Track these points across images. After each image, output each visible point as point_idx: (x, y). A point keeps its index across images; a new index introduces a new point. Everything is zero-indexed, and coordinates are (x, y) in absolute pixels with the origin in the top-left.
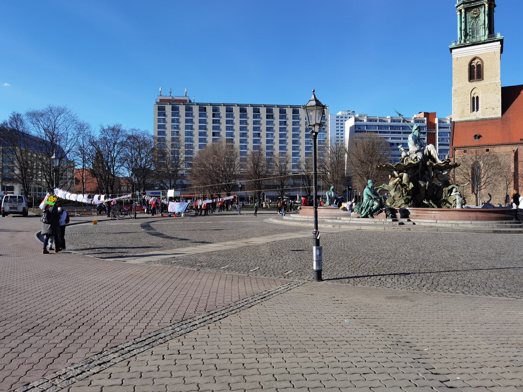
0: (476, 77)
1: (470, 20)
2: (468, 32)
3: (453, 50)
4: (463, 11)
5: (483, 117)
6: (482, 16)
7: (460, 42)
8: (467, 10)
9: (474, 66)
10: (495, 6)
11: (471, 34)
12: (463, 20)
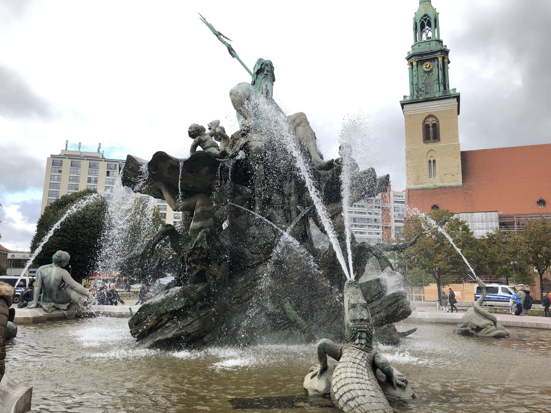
1: (422, 74)
3: (405, 106)
4: (415, 63)
5: (441, 185)
10: (449, 62)
11: (423, 89)
12: (415, 73)
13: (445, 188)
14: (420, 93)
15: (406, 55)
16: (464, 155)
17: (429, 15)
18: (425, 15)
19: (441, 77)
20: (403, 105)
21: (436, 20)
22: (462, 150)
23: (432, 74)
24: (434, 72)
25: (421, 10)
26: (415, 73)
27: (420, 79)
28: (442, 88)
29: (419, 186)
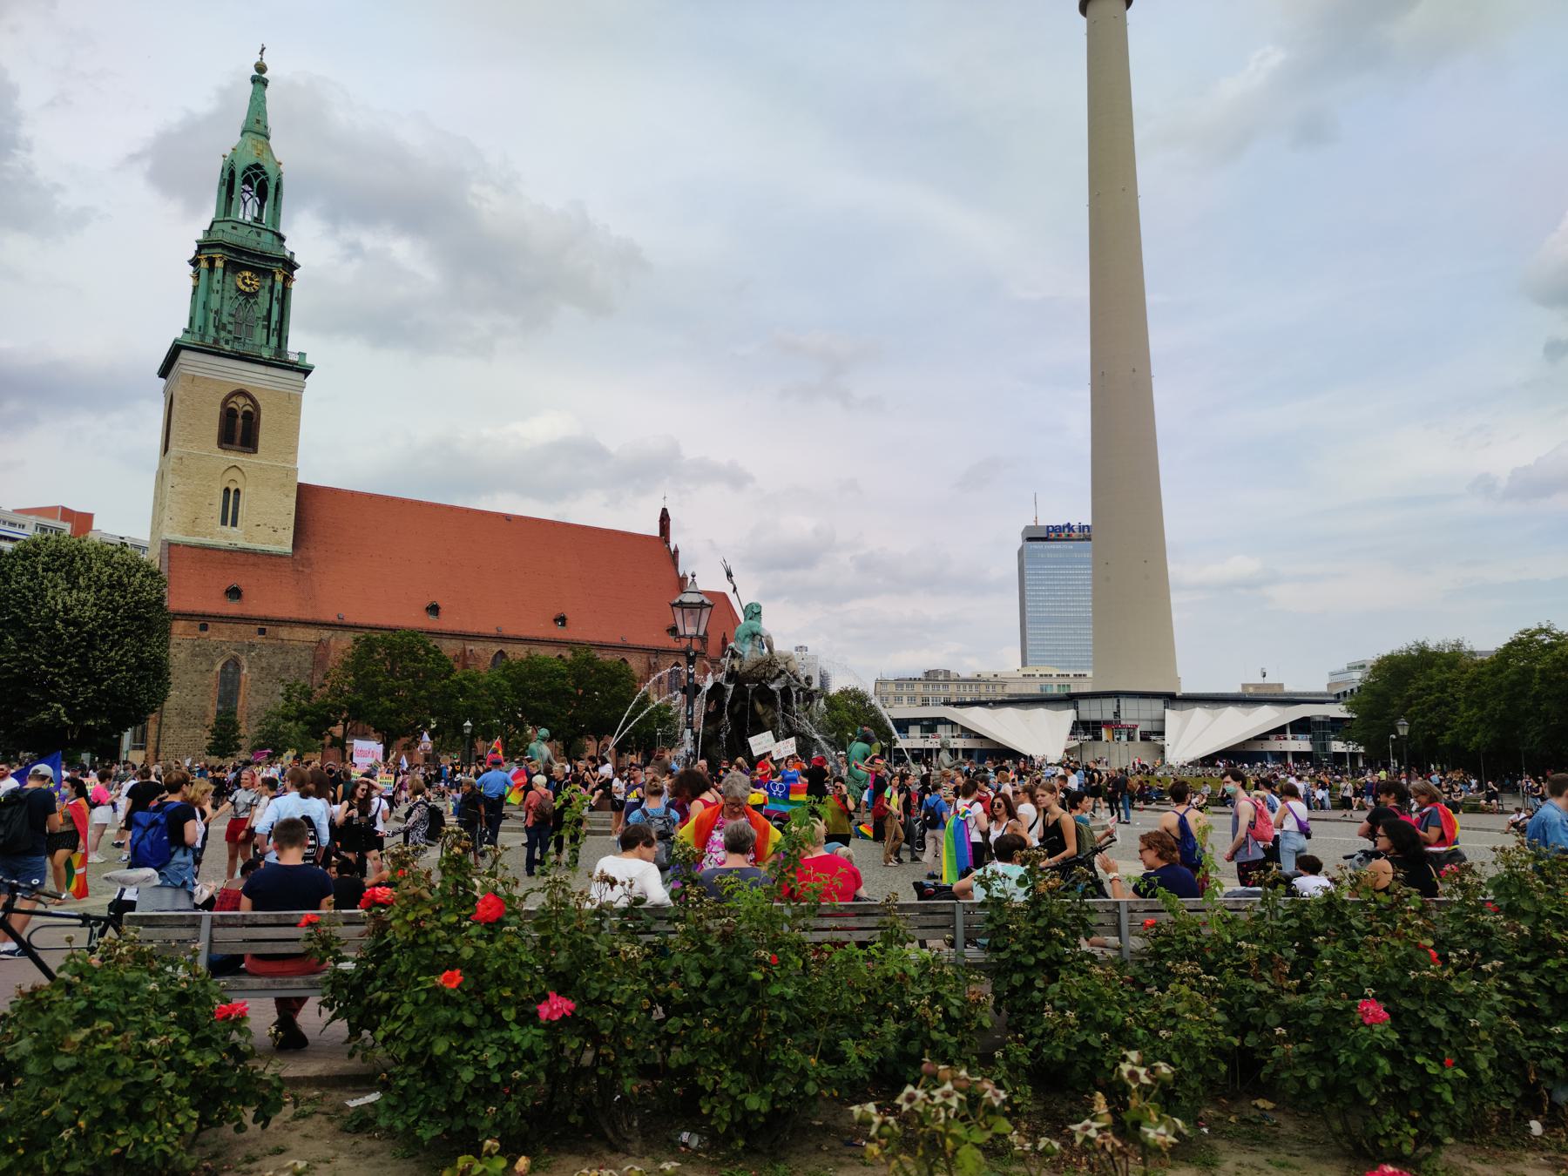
0: (238, 441)
1: (233, 293)
4: (219, 264)
6: (264, 298)
11: (230, 327)
13: (254, 553)
14: (223, 334)
15: (201, 237)
16: (304, 492)
17: (266, 168)
18: (258, 166)
19: (275, 317)
20: (176, 350)
21: (278, 187)
22: (301, 479)
24: (260, 300)
25: (249, 148)
26: (216, 286)
27: (226, 302)
28: (274, 341)
29: (193, 540)
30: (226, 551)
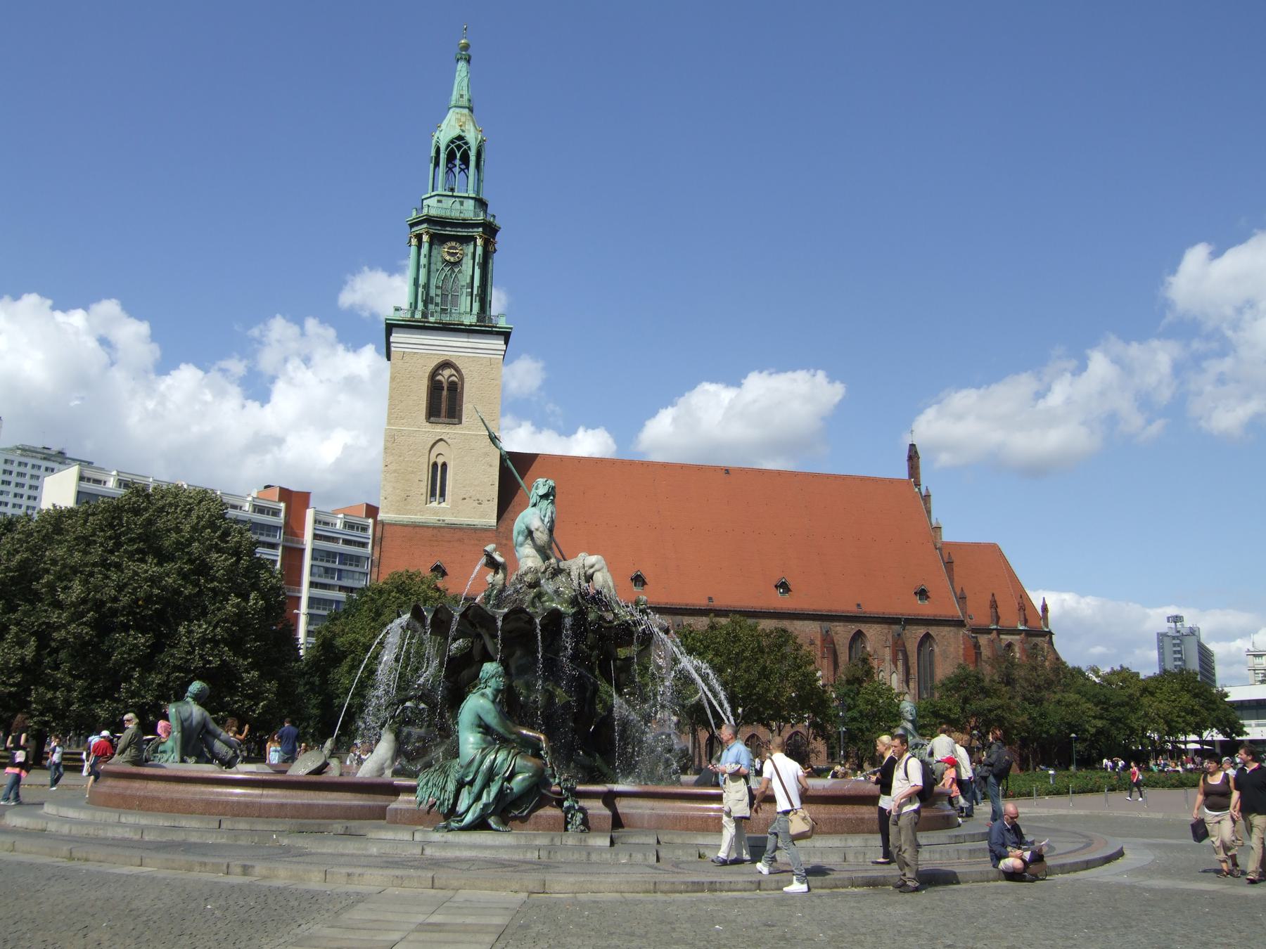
1: (440, 266)
2: (432, 293)
4: (425, 238)
6: (467, 264)
7: (413, 314)
8: (437, 240)
9: (440, 382)
11: (438, 300)
12: (423, 261)
18: (460, 138)
19: (477, 283)
23: (460, 271)
26: (423, 261)
28: (476, 306)
30: (434, 527)
